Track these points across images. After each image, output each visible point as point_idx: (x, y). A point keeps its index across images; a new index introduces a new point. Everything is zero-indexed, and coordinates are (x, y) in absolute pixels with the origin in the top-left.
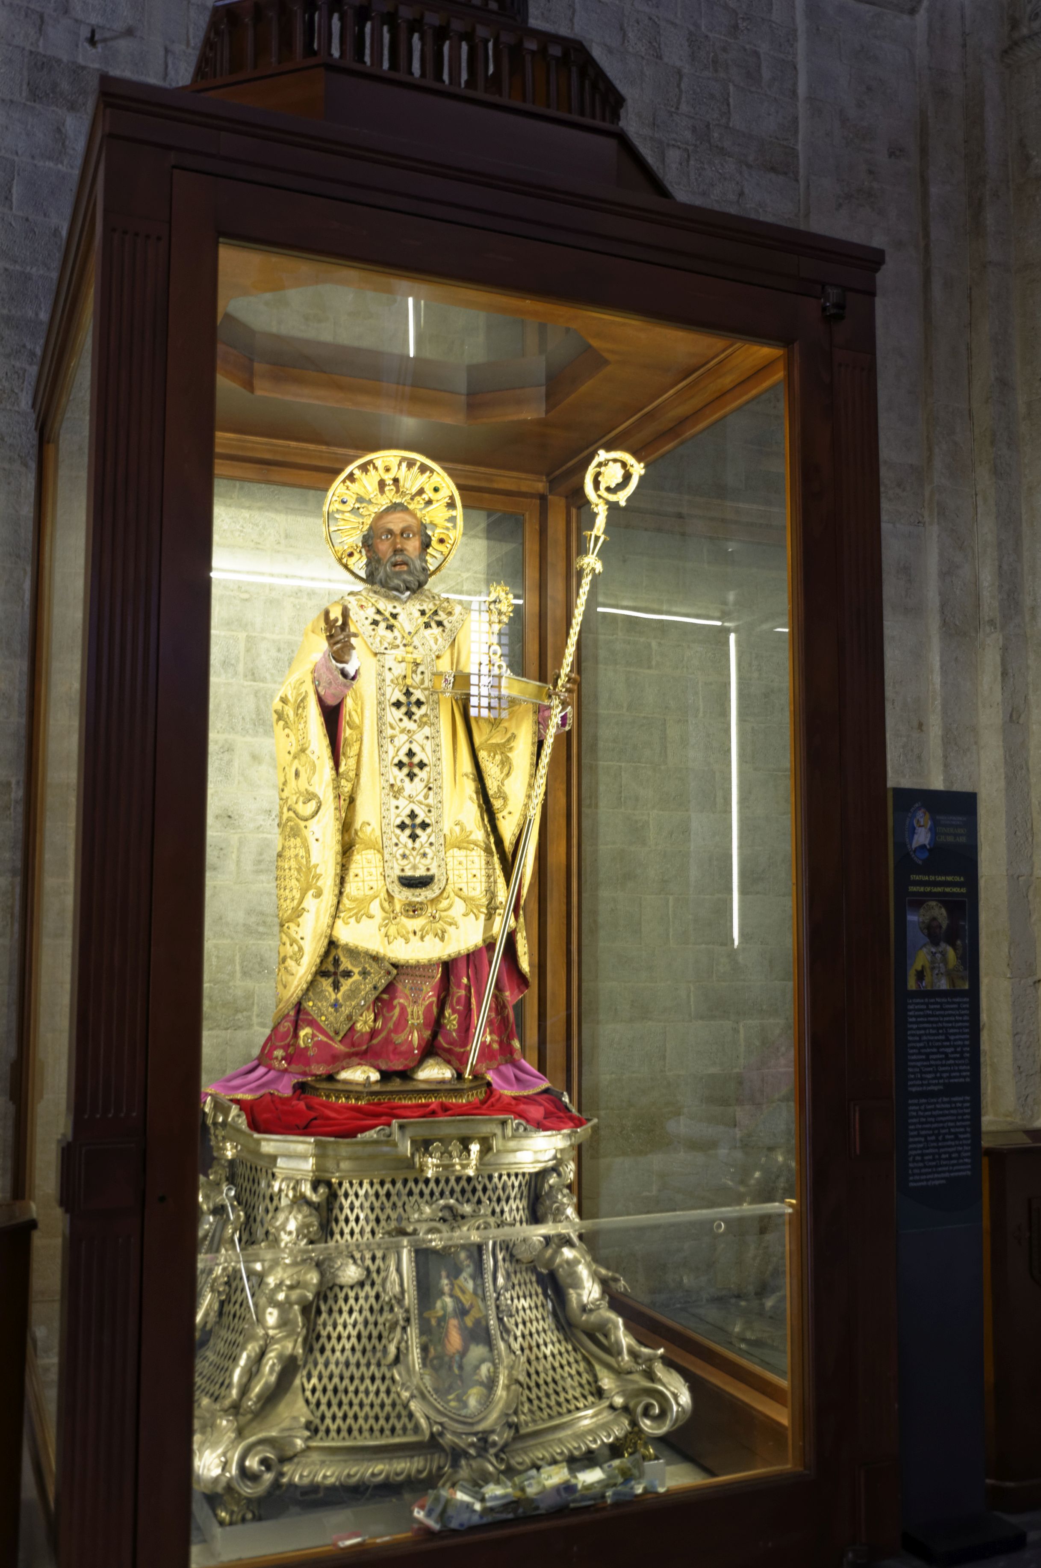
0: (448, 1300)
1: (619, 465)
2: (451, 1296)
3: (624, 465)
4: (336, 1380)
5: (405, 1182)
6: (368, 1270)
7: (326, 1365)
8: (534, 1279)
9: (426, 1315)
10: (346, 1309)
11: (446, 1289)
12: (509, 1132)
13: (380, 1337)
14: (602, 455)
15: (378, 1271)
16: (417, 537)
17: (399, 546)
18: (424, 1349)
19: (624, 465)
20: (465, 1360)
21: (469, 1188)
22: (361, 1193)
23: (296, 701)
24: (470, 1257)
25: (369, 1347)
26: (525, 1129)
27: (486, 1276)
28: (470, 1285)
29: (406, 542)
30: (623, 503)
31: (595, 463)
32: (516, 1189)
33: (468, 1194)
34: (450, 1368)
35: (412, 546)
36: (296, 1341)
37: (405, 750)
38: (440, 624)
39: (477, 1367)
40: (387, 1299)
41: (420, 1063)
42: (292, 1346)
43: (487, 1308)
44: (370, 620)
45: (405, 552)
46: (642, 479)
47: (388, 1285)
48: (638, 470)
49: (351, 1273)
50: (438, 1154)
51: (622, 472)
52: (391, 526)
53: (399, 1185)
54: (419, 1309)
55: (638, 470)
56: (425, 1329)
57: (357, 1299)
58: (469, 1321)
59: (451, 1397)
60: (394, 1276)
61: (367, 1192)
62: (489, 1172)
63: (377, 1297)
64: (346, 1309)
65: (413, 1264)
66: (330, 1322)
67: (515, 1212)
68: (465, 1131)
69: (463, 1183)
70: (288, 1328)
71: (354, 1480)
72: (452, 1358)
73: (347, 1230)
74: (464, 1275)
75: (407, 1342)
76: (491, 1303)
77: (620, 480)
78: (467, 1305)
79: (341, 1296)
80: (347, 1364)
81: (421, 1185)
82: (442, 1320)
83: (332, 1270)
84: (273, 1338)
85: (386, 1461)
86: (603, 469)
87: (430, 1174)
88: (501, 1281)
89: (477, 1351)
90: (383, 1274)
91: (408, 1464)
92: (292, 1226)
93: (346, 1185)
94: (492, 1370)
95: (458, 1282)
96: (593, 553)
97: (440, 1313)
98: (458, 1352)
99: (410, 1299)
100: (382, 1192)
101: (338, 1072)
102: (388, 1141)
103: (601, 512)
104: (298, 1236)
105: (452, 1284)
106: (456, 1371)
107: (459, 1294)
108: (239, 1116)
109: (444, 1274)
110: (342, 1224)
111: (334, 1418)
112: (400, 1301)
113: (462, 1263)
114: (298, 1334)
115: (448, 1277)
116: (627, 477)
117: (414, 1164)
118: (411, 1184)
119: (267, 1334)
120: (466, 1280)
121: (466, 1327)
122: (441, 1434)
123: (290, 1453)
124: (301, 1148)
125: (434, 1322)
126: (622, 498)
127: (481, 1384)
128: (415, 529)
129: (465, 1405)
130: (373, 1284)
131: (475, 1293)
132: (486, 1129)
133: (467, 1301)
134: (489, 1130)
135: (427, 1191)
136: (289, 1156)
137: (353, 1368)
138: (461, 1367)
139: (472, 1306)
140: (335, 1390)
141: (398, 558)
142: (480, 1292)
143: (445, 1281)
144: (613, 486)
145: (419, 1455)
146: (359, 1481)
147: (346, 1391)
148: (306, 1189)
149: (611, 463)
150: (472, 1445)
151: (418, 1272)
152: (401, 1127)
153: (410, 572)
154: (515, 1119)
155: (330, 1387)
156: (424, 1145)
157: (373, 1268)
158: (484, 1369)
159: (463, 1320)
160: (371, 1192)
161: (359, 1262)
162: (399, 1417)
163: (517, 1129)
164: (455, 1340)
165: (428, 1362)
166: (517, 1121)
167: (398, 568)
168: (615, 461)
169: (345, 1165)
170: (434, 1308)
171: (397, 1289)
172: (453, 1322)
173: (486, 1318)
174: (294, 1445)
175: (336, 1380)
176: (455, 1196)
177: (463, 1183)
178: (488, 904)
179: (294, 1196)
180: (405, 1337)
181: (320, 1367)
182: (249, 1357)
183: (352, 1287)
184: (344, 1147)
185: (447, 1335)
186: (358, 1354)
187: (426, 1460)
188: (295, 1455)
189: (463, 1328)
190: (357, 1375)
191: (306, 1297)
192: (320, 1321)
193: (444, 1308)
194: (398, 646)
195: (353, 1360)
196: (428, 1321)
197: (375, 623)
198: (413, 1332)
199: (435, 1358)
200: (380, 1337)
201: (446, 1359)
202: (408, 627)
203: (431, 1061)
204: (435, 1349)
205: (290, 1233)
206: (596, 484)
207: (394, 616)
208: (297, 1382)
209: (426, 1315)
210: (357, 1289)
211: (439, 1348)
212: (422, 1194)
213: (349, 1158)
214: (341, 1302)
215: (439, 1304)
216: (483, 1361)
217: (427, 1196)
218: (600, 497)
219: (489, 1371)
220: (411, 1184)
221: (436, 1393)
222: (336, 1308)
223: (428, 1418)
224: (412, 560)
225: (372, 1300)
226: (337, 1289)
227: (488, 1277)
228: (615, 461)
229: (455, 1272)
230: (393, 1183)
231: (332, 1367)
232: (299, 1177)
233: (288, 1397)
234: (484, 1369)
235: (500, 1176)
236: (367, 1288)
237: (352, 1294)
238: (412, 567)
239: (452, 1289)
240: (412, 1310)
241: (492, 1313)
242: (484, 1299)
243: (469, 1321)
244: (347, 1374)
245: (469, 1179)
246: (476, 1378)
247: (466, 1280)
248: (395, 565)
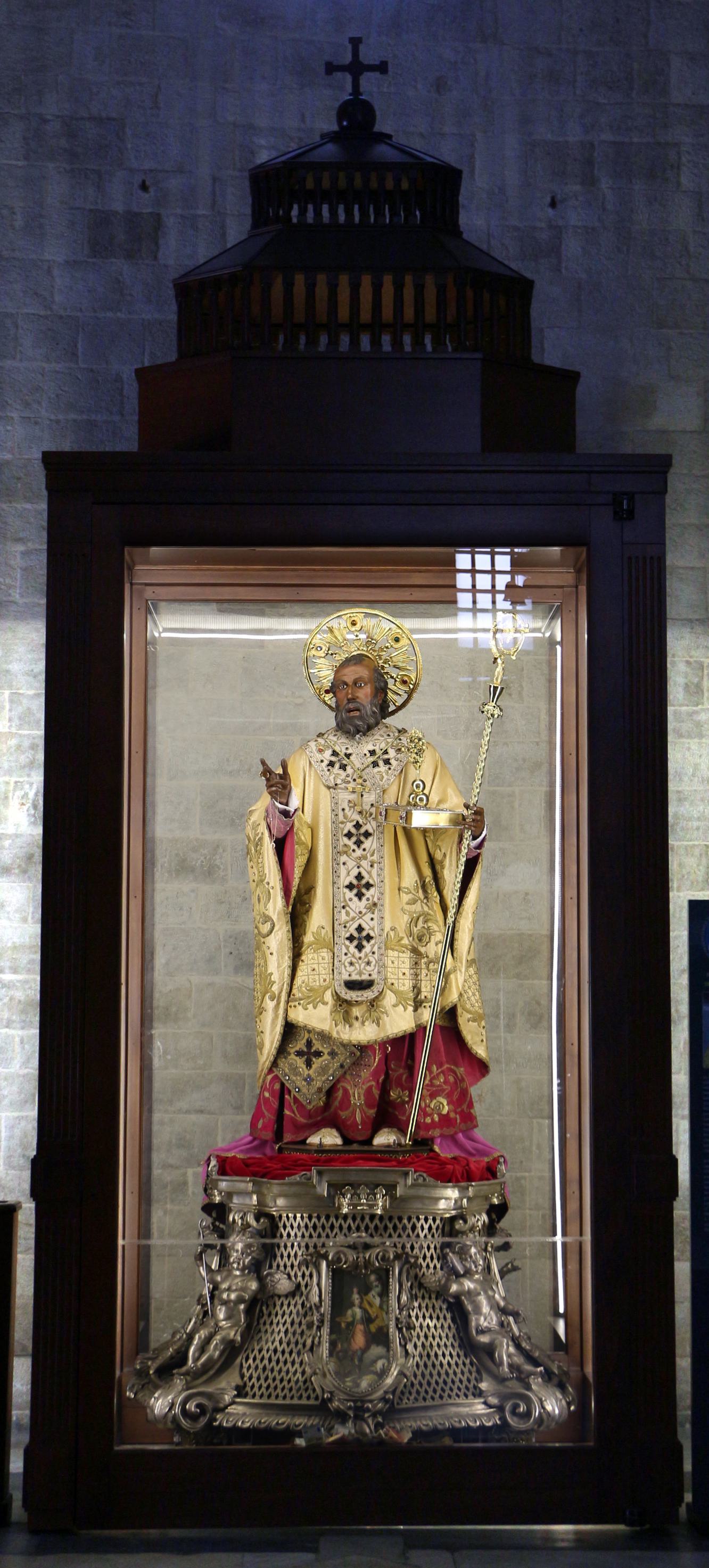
0: (358, 1311)
2: (360, 1307)
4: (266, 1362)
5: (328, 1218)
6: (298, 1286)
7: (260, 1351)
8: (444, 1307)
9: (337, 1319)
10: (280, 1312)
11: (357, 1302)
12: (410, 1182)
13: (302, 1333)
15: (306, 1286)
16: (369, 685)
17: (350, 696)
18: (333, 1344)
20: (365, 1355)
21: (381, 1226)
22: (295, 1225)
23: (255, 839)
24: (379, 1279)
25: (293, 1340)
26: (424, 1180)
27: (391, 1295)
28: (377, 1301)
29: (360, 690)
32: (426, 1231)
33: (381, 1231)
34: (352, 1360)
36: (237, 1331)
37: (355, 872)
38: (387, 762)
39: (375, 1362)
40: (308, 1306)
41: (375, 1131)
42: (234, 1335)
43: (389, 1320)
44: (326, 762)
45: (358, 700)
47: (310, 1296)
49: (283, 1284)
50: (349, 1196)
52: (346, 679)
53: (323, 1220)
54: (331, 1314)
56: (334, 1328)
57: (289, 1305)
58: (373, 1328)
59: (348, 1379)
60: (316, 1289)
61: (299, 1224)
62: (400, 1214)
63: (303, 1304)
64: (280, 1312)
65: (330, 1281)
66: (268, 1322)
67: (426, 1249)
68: (371, 1178)
69: (377, 1221)
70: (233, 1321)
71: (263, 1426)
72: (355, 1352)
73: (285, 1254)
74: (373, 1293)
75: (320, 1338)
76: (392, 1317)
78: (373, 1316)
79: (279, 1303)
80: (275, 1351)
81: (341, 1221)
82: (351, 1325)
83: (273, 1284)
84: (220, 1327)
85: (290, 1417)
87: (345, 1210)
88: (404, 1298)
89: (376, 1350)
90: (309, 1288)
91: (306, 1420)
92: (239, 1246)
93: (284, 1218)
94: (386, 1365)
95: (367, 1297)
97: (350, 1319)
98: (360, 1348)
99: (326, 1308)
100: (310, 1225)
101: (306, 1139)
102: (308, 1183)
104: (242, 1254)
105: (362, 1299)
106: (357, 1362)
107: (367, 1307)
108: (215, 1166)
109: (355, 1290)
110: (282, 1249)
111: (260, 1387)
112: (318, 1307)
113: (371, 1283)
114: (240, 1326)
115: (359, 1293)
117: (334, 1204)
118: (333, 1219)
119: (216, 1325)
120: (374, 1297)
121: (370, 1332)
122: (330, 1400)
123: (222, 1405)
124: (242, 1186)
125: (343, 1325)
127: (376, 1373)
128: (367, 680)
129: (358, 1385)
130: (302, 1295)
131: (381, 1307)
132: (390, 1178)
133: (373, 1312)
134: (392, 1179)
135: (345, 1226)
136: (241, 1193)
137: (279, 1354)
138: (361, 1360)
139: (377, 1317)
140: (264, 1369)
141: (351, 706)
142: (385, 1307)
143: (356, 1297)
145: (316, 1416)
146: (267, 1427)
147: (272, 1370)
148: (250, 1219)
150: (350, 1408)
151: (333, 1287)
152: (320, 1173)
153: (361, 718)
154: (416, 1171)
155: (261, 1366)
156: (337, 1188)
157: (303, 1283)
158: (379, 1364)
159: (368, 1326)
160: (302, 1225)
161: (293, 1279)
162: (306, 1390)
163: (417, 1179)
164: (359, 1340)
165: (335, 1354)
166: (418, 1174)
167: (352, 714)
169: (280, 1202)
170: (345, 1315)
171: (317, 1299)
172: (360, 1328)
173: (388, 1327)
174: (224, 1400)
175: (266, 1362)
176: (370, 1231)
177: (377, 1221)
178: (415, 998)
179: (242, 1224)
180: (319, 1334)
181: (256, 1352)
182: (200, 1338)
183: (286, 1296)
184: (275, 1187)
185: (353, 1336)
186: (284, 1345)
187: (320, 1420)
188: (226, 1407)
189: (367, 1333)
190: (282, 1359)
191: (243, 1296)
192: (262, 1321)
193: (354, 1316)
194: (350, 782)
195: (280, 1349)
196: (340, 1324)
197: (331, 764)
198: (325, 1330)
199: (340, 1351)
200: (302, 1333)
201: (350, 1353)
202: (358, 765)
203: (386, 1130)
204: (342, 1345)
205: (237, 1251)
207: (348, 756)
208: (238, 1361)
209: (337, 1319)
210: (290, 1299)
211: (345, 1345)
212: (341, 1228)
213: (280, 1195)
214: (278, 1308)
215: (349, 1312)
216: (380, 1358)
217: (345, 1230)
219: (383, 1365)
220: (333, 1219)
221: (336, 1376)
222: (274, 1312)
223: (323, 1389)
224: (363, 706)
225: (299, 1307)
226: (276, 1299)
227: (393, 1296)
229: (365, 1290)
230: (319, 1218)
231: (264, 1352)
232: (246, 1210)
233: (230, 1371)
234: (379, 1364)
235: (409, 1219)
236: (297, 1298)
237: (286, 1302)
239: (361, 1302)
240: (326, 1314)
241: (392, 1324)
242: (387, 1313)
243: (373, 1328)
244: (274, 1358)
245: (381, 1218)
246: (373, 1369)
247: (374, 1297)
248: (350, 711)
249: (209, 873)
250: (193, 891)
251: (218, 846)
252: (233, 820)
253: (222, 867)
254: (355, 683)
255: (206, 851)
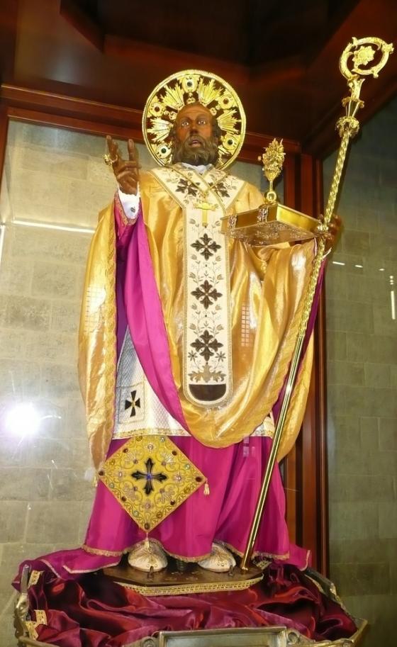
1: (370, 47)
3: (374, 47)
14: (356, 42)
17: (194, 128)
19: (374, 47)
30: (376, 75)
31: (349, 46)
35: (205, 132)
46: (391, 56)
48: (388, 48)
51: (374, 52)
55: (388, 48)
77: (371, 58)
86: (355, 52)
96: (351, 115)
103: (356, 89)
116: (378, 56)
126: (375, 71)
144: (366, 63)
149: (362, 47)
168: (366, 45)
206: (350, 64)
218: (353, 73)
228: (366, 45)
238: (204, 144)
249: (36, 322)
250: (23, 334)
251: (44, 305)
252: (56, 288)
253: (45, 319)
254: (198, 120)
255: (35, 307)
